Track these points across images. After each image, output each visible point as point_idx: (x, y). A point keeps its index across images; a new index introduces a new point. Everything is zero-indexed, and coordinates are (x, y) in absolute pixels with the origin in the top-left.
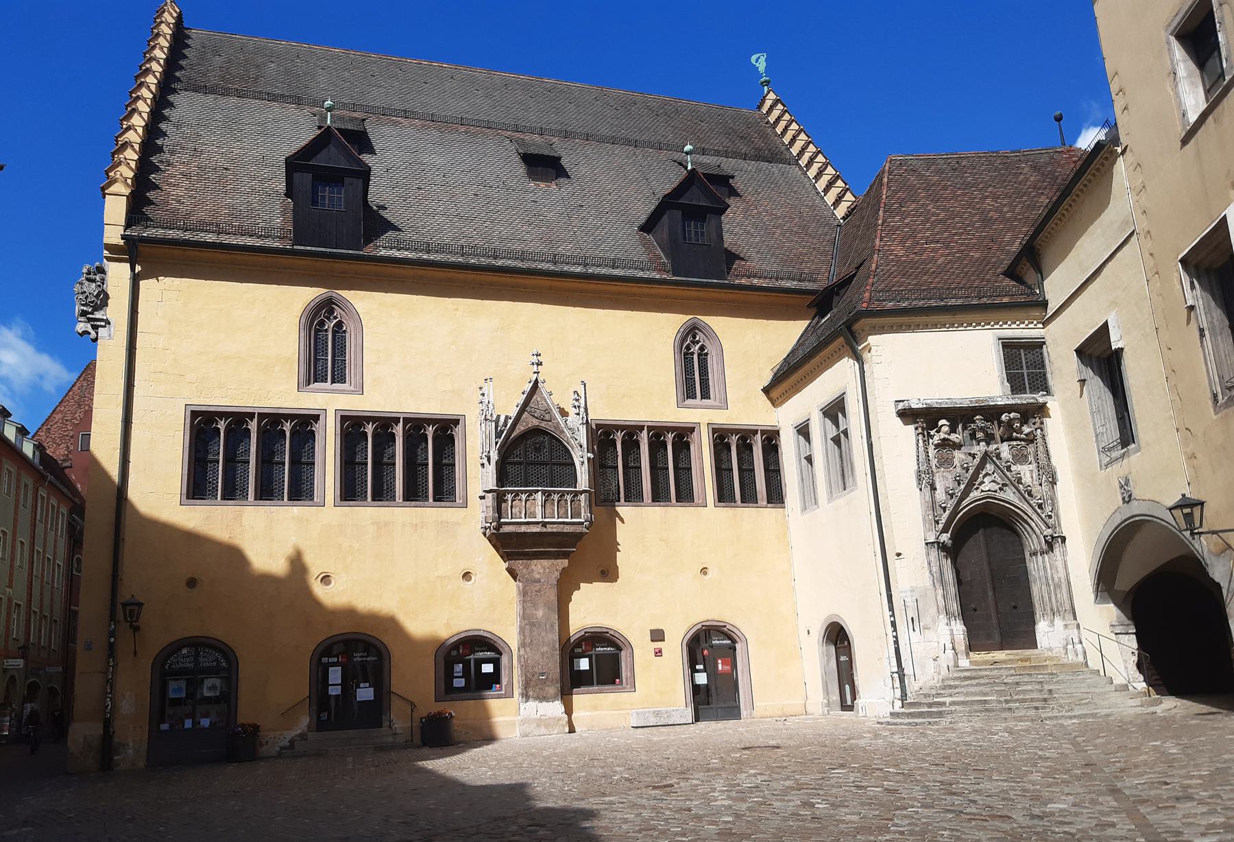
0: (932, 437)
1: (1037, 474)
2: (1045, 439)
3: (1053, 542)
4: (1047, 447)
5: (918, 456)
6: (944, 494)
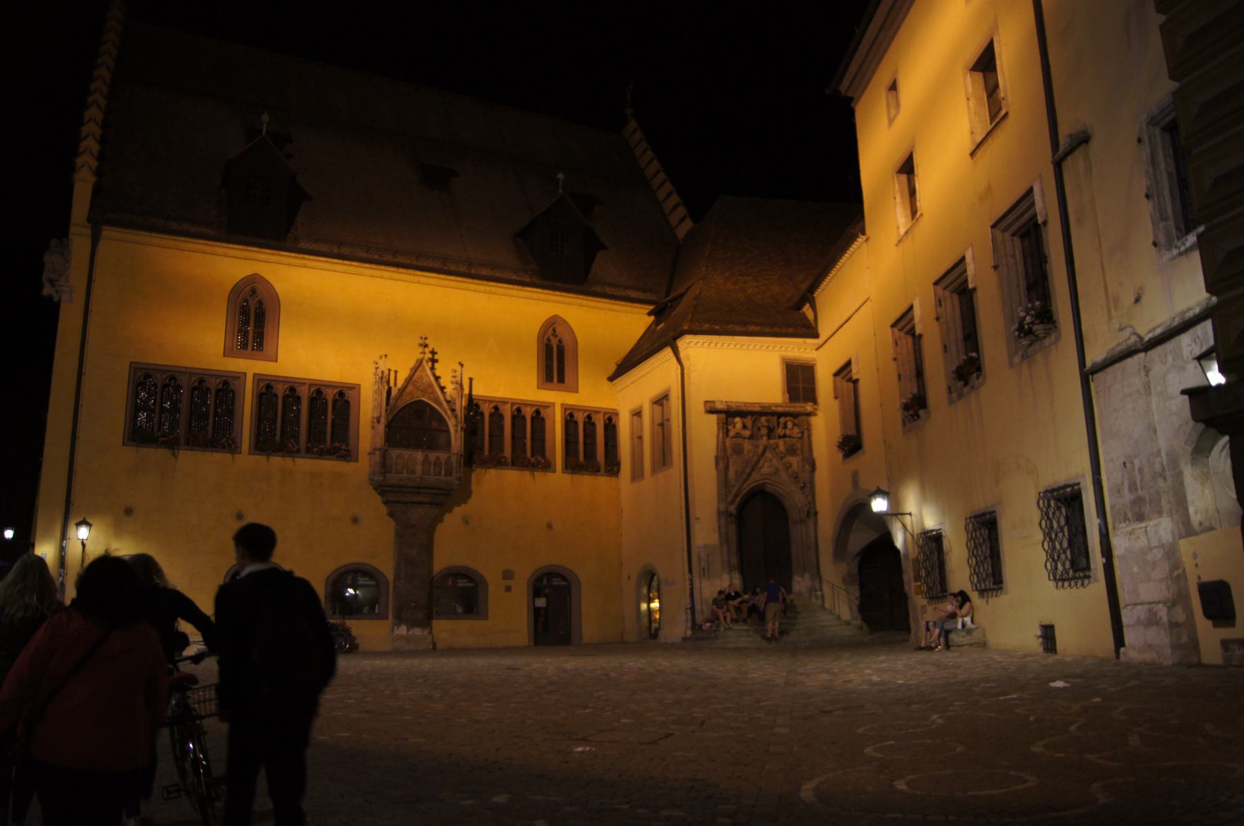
3: (812, 513)
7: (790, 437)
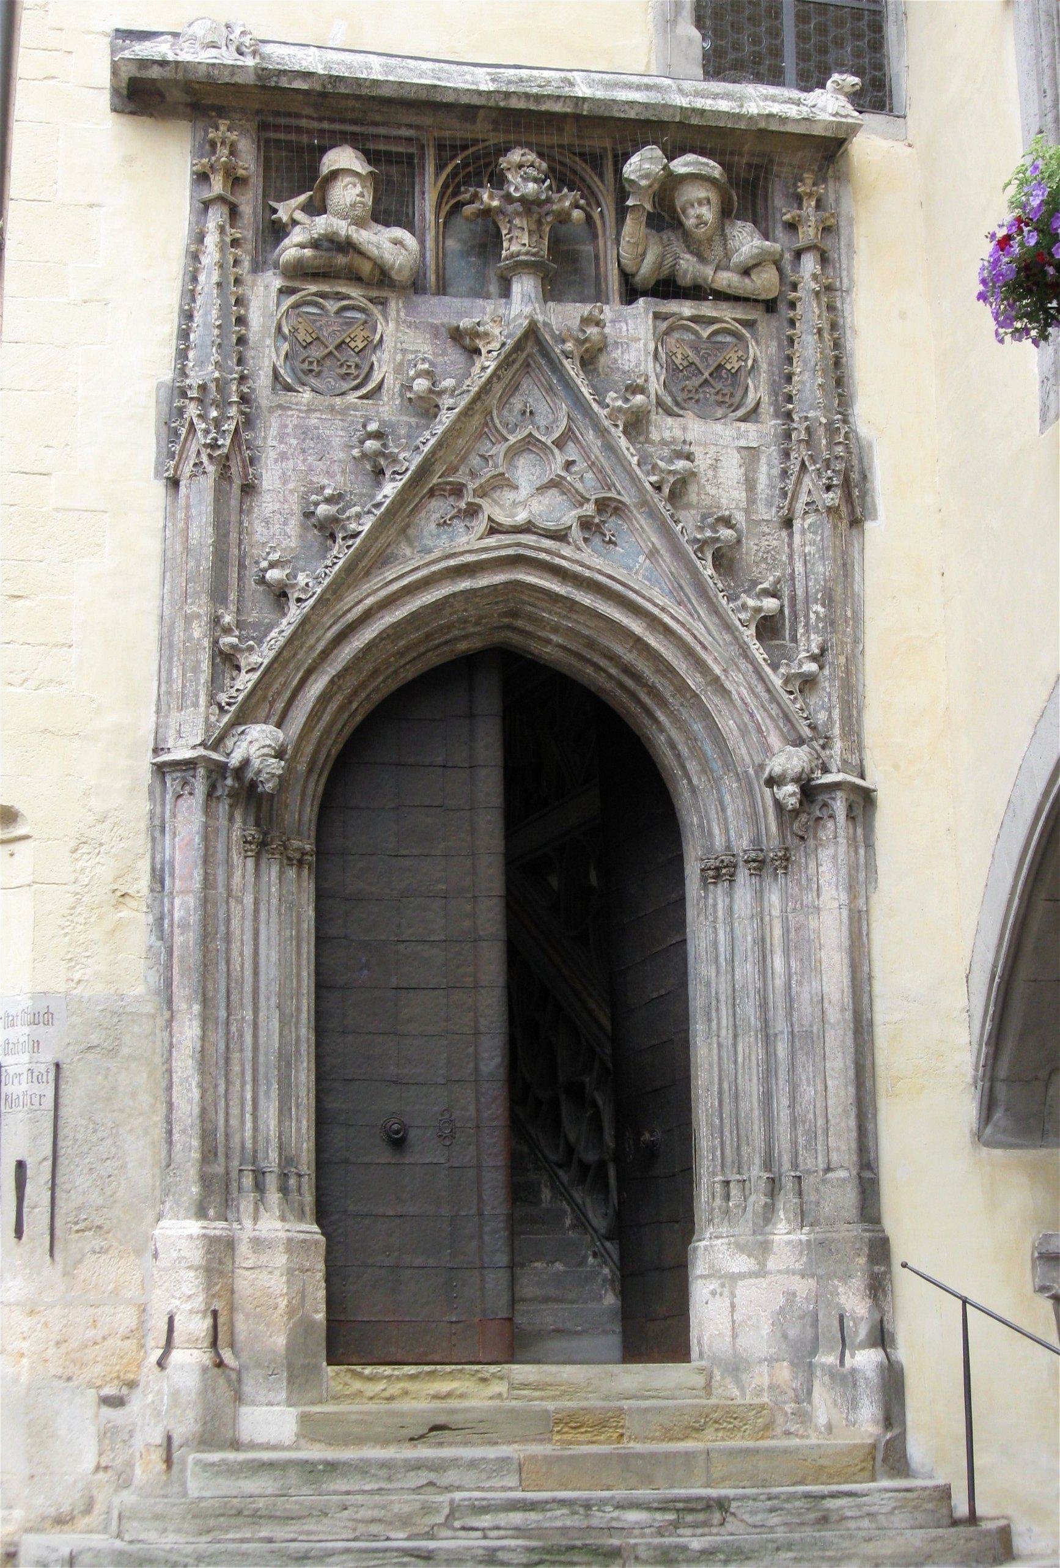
0: (277, 231)
1: (776, 472)
2: (831, 308)
4: (837, 345)
5: (188, 316)
6: (294, 523)
7: (697, 292)
